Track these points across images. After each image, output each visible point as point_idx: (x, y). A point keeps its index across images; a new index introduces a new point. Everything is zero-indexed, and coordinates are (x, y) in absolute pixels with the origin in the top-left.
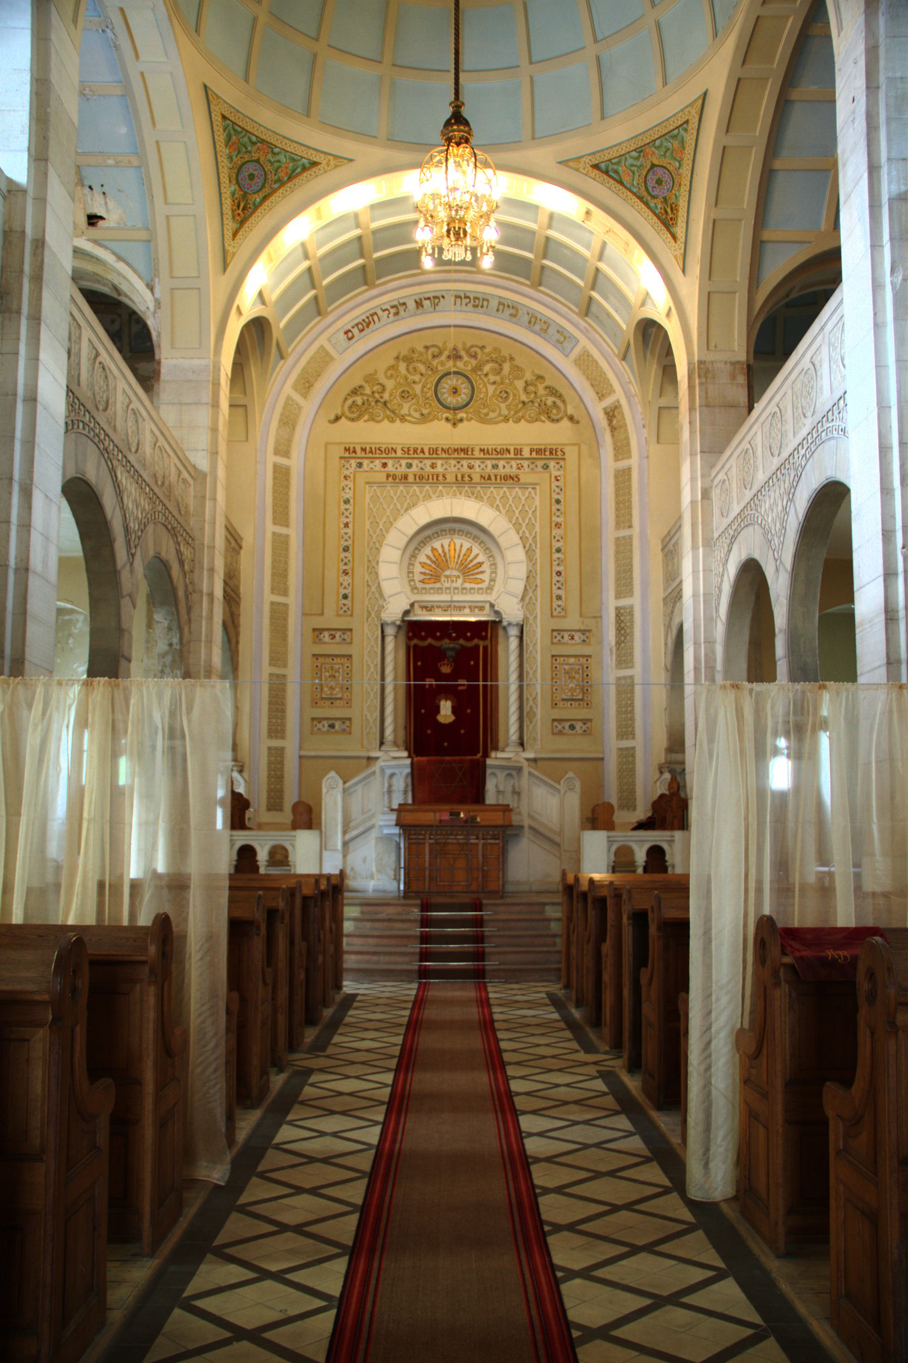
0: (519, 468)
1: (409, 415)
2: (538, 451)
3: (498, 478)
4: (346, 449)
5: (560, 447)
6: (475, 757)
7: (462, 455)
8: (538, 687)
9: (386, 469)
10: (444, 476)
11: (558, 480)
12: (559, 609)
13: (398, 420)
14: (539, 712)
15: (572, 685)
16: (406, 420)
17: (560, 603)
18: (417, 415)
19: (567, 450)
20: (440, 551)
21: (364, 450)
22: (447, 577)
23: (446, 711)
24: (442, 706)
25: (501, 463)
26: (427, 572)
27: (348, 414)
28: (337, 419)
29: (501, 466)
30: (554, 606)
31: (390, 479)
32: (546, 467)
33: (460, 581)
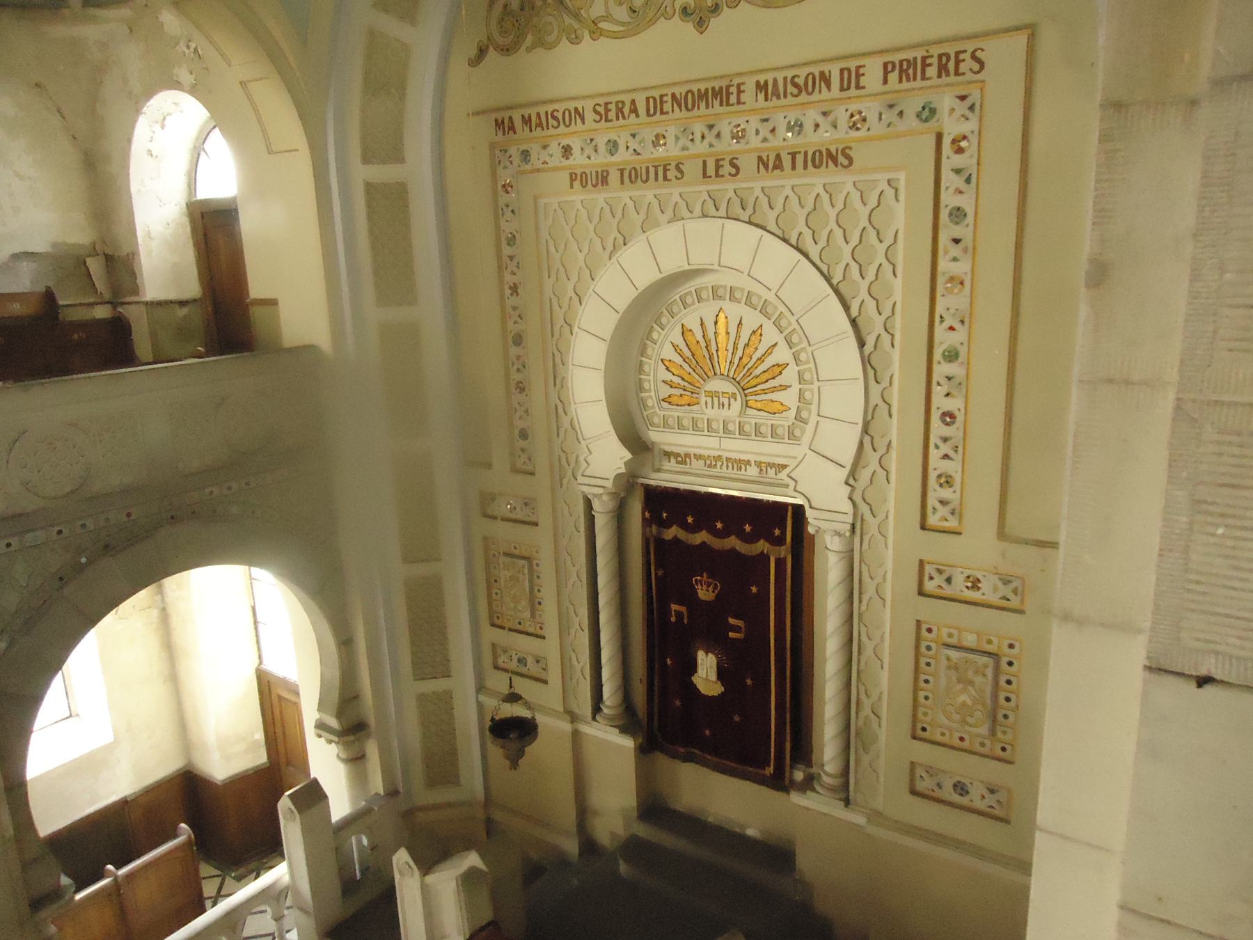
0: (854, 127)
1: (607, 17)
2: (908, 70)
3: (800, 159)
4: (499, 124)
5: (970, 46)
6: (761, 772)
7: (717, 108)
8: (884, 676)
9: (571, 162)
10: (678, 168)
11: (960, 151)
12: (943, 511)
13: (586, 33)
14: (883, 734)
15: (963, 698)
16: (602, 33)
17: (946, 493)
18: (621, 13)
19: (993, 51)
20: (699, 336)
21: (527, 121)
22: (711, 394)
23: (706, 672)
24: (699, 661)
25: (812, 116)
26: (677, 380)
27: (500, 40)
28: (482, 52)
29: (808, 127)
30: (932, 502)
31: (577, 184)
32: (928, 113)
33: (737, 405)
